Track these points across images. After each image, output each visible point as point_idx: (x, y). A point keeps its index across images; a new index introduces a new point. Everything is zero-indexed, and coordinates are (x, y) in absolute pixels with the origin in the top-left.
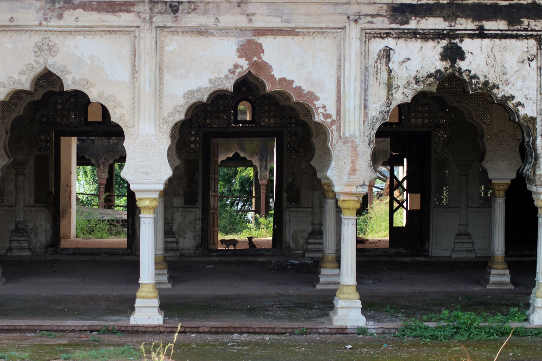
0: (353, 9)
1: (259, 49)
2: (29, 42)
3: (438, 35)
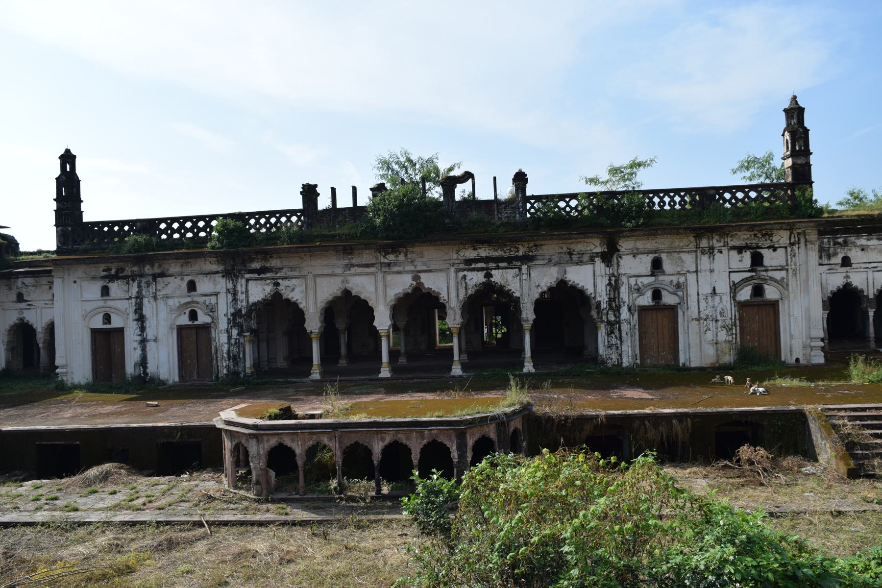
0: (452, 262)
1: (419, 278)
2: (339, 280)
3: (482, 269)
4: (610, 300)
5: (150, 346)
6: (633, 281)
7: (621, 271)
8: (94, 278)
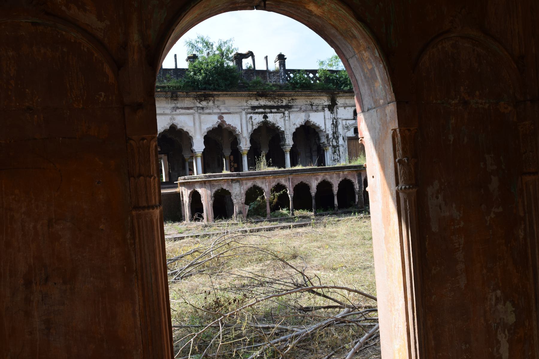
0: (243, 107)
1: (223, 117)
2: (168, 118)
3: (262, 113)
4: (334, 133)
6: (344, 122)
7: (339, 116)
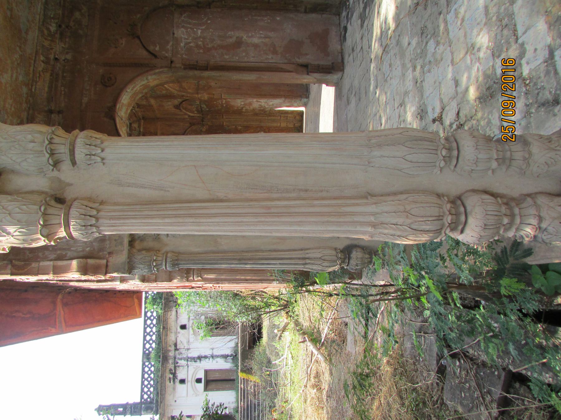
5: (216, 353)
8: (174, 389)
